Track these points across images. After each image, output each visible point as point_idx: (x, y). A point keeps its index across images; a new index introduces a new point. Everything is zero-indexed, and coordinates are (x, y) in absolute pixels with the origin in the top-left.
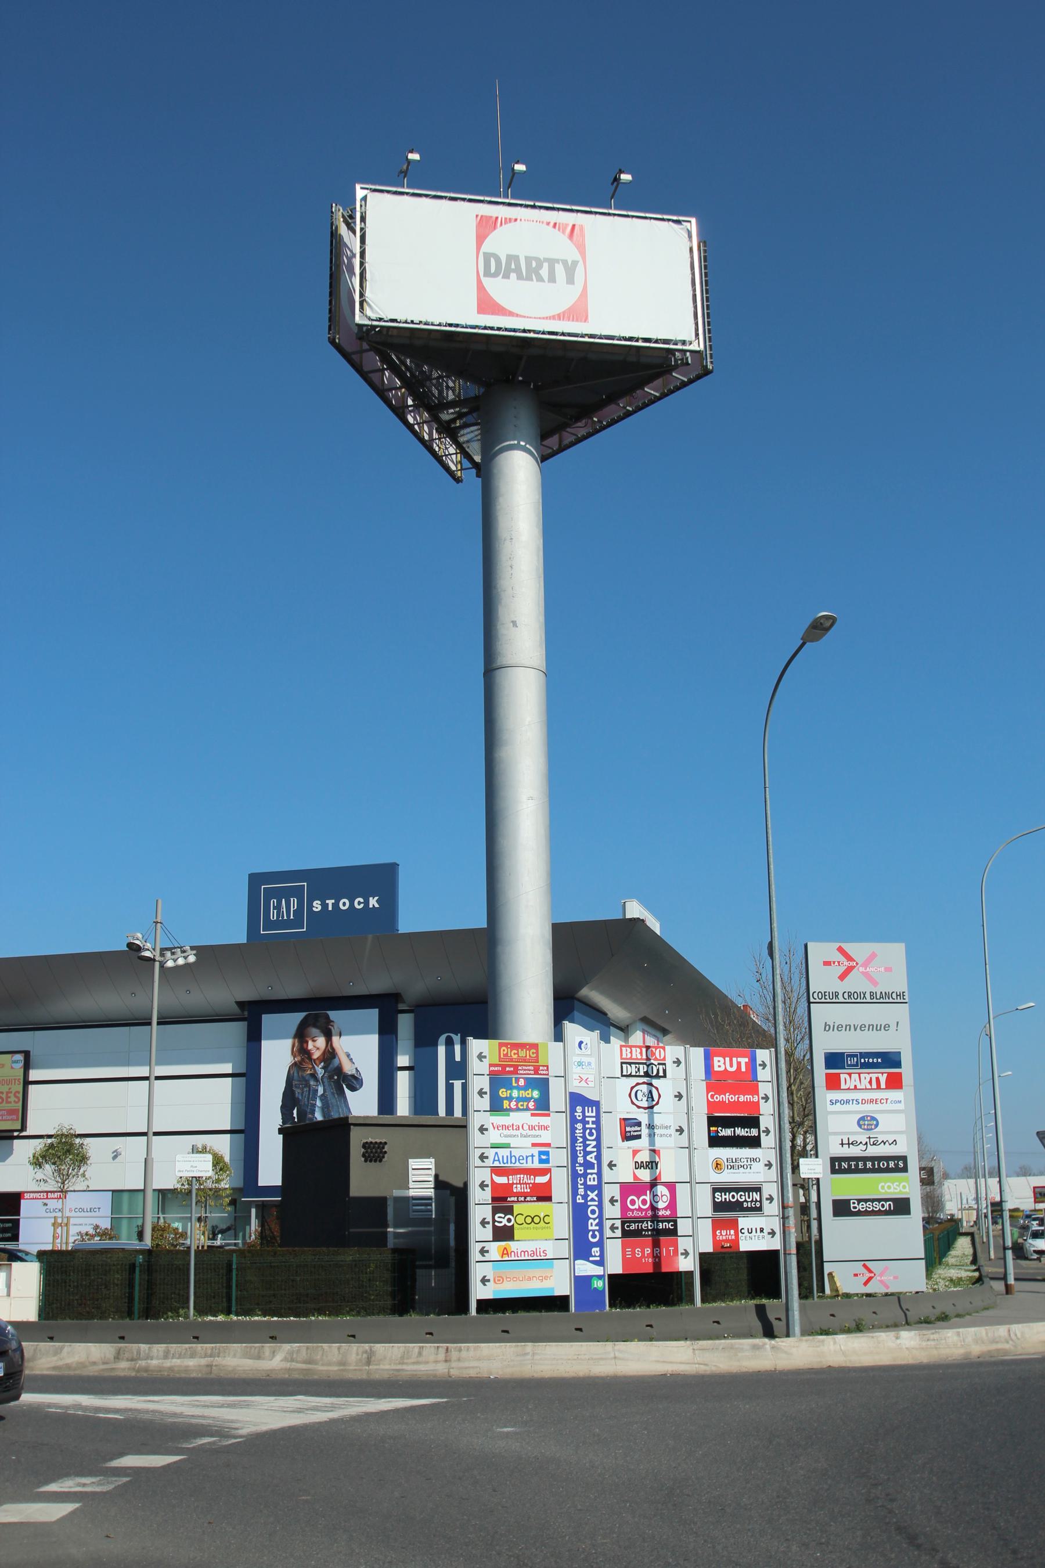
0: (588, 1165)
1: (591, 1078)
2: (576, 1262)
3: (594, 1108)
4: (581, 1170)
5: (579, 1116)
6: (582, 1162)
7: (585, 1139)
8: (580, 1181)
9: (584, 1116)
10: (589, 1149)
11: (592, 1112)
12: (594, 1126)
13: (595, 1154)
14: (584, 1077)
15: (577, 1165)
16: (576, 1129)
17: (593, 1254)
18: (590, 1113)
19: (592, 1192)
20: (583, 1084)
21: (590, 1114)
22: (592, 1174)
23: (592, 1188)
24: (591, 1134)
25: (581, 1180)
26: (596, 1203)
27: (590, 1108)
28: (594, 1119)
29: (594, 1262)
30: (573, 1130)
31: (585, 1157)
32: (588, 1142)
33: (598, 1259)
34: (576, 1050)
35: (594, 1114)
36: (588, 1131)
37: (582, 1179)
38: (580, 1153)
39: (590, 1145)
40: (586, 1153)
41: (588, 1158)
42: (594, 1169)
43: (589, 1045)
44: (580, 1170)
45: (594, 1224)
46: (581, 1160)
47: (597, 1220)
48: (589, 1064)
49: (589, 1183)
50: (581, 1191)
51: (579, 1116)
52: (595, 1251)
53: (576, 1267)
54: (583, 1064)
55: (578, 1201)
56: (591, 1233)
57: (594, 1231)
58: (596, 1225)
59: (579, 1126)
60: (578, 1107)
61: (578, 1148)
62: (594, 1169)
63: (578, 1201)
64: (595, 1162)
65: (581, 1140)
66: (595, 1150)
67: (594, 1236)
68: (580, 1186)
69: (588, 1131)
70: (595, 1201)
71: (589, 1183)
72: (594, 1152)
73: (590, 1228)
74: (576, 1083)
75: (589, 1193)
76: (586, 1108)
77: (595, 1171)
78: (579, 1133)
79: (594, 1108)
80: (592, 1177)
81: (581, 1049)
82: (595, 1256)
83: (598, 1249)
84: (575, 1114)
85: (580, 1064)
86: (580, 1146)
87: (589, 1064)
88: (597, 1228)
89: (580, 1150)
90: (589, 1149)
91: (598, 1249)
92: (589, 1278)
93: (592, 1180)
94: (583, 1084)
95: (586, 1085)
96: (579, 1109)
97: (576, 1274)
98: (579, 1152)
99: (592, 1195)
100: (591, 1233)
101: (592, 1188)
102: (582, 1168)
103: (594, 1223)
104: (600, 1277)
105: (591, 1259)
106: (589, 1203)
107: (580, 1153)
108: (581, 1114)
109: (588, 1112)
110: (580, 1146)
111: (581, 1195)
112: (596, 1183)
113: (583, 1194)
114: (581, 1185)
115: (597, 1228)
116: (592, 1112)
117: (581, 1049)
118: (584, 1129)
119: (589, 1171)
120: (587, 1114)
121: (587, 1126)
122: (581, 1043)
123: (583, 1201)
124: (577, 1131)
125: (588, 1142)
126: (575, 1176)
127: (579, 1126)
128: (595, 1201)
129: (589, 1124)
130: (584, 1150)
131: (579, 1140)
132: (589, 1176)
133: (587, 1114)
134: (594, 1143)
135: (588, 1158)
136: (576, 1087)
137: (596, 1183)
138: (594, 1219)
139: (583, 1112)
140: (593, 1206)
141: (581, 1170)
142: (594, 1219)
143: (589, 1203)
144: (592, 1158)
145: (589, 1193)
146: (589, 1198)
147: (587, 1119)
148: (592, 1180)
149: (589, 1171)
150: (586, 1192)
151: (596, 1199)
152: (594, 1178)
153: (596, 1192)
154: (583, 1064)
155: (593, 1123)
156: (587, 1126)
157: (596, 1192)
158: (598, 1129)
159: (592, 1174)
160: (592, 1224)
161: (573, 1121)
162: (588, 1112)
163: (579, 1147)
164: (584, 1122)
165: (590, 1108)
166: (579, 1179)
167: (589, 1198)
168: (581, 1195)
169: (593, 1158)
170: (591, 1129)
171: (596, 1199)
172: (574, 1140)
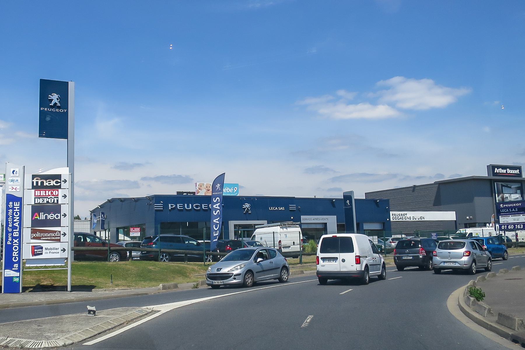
0: (14, 228)
1: (18, 187)
2: (5, 271)
3: (19, 202)
4: (10, 230)
5: (11, 206)
6: (11, 226)
7: (13, 216)
8: (10, 235)
9: (13, 206)
10: (15, 221)
11: (18, 204)
12: (19, 210)
13: (18, 222)
14: (14, 187)
15: (8, 228)
16: (9, 212)
17: (15, 267)
18: (17, 205)
19: (16, 240)
20: (14, 190)
21: (17, 205)
22: (16, 231)
23: (16, 238)
24: (17, 214)
25: (10, 234)
26: (18, 244)
27: (17, 203)
28: (19, 207)
29: (14, 270)
30: (7, 212)
31: (13, 224)
32: (14, 218)
33: (17, 269)
34: (11, 174)
35: (19, 205)
36: (15, 213)
37: (11, 234)
38: (10, 223)
39: (16, 219)
40: (13, 223)
41: (14, 225)
42: (17, 229)
43: (18, 172)
44: (10, 230)
45: (15, 254)
46: (10, 225)
47: (17, 252)
48: (17, 180)
49: (14, 236)
50: (10, 239)
51: (11, 206)
52: (16, 265)
53: (5, 273)
54: (14, 180)
55: (8, 244)
56: (14, 258)
57: (15, 257)
58: (17, 254)
59: (11, 211)
60: (11, 202)
61: (9, 220)
62: (17, 229)
63: (8, 244)
64: (18, 226)
65: (11, 217)
66: (18, 221)
67: (15, 259)
68: (9, 237)
69: (15, 213)
70: (17, 243)
71: (14, 236)
72: (18, 222)
73: (13, 255)
74: (10, 190)
75: (14, 240)
76: (15, 203)
77: (18, 230)
78: (10, 213)
79: (19, 202)
80: (16, 233)
81: (14, 174)
82: (16, 268)
83: (17, 265)
84: (9, 205)
85: (12, 181)
86: (10, 220)
87: (17, 180)
88: (17, 255)
89: (10, 221)
90: (15, 221)
91: (17, 265)
92: (11, 278)
93: (16, 234)
94: (14, 190)
95: (16, 191)
96: (11, 203)
97: (5, 276)
98: (9, 222)
99: (15, 241)
100: (14, 258)
101: (16, 238)
102: (11, 229)
103: (16, 253)
104: (17, 277)
105: (13, 269)
106: (14, 245)
107: (10, 223)
108: (12, 205)
109: (16, 204)
110: (10, 220)
111: (10, 241)
112: (18, 235)
113: (10, 240)
114: (10, 236)
115: (17, 255)
116: (18, 204)
117: (14, 174)
118: (13, 212)
119: (14, 230)
120: (15, 205)
121: (15, 210)
122: (14, 171)
123: (11, 244)
124: (9, 213)
125: (14, 218)
126: (7, 232)
127: (11, 211)
128: (17, 243)
129: (16, 209)
130: (13, 221)
131: (10, 217)
132: (14, 233)
133: (15, 205)
134: (18, 218)
135: (14, 225)
136: (10, 191)
137: (18, 235)
138: (16, 252)
139: (13, 204)
140: (16, 246)
141: (10, 230)
142: (16, 252)
143: (14, 245)
144: (16, 224)
145: (14, 240)
146: (14, 242)
147: (15, 207)
148: (16, 234)
149: (14, 230)
150: (12, 240)
151: (18, 242)
152: (17, 234)
153: (18, 240)
154: (14, 180)
155: (18, 209)
156: (15, 210)
157: (18, 240)
158: (20, 212)
159: (16, 231)
160: (15, 254)
161: (8, 208)
162: (16, 204)
163: (10, 220)
164: (13, 209)
165: (17, 203)
166: (9, 234)
167: (14, 242)
168: (10, 241)
169: (17, 224)
170: (17, 212)
171: (18, 242)
172: (7, 217)
